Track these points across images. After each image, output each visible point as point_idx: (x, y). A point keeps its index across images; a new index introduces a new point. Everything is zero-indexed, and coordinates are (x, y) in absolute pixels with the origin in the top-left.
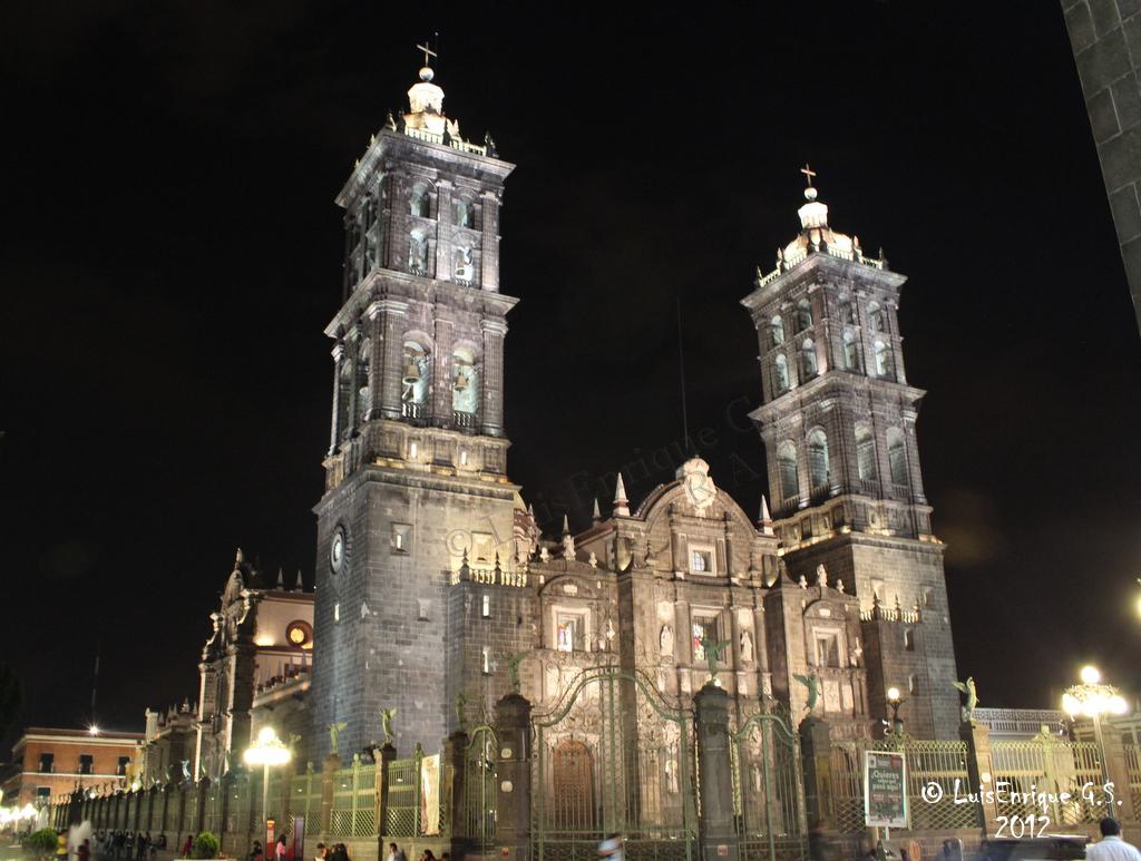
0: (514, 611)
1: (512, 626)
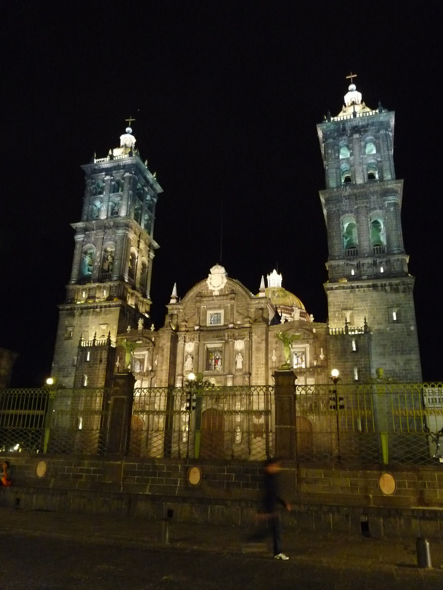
0: (99, 357)
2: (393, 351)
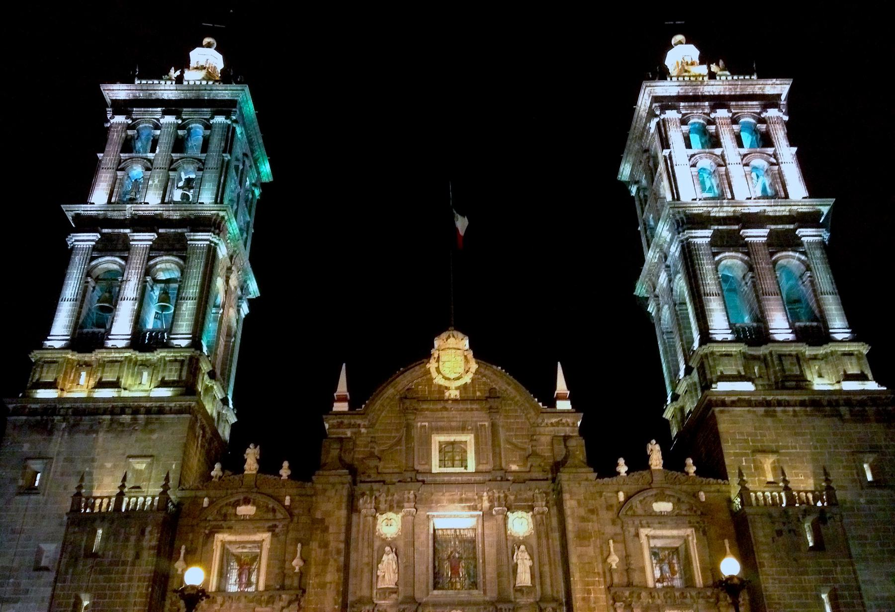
1: (124, 563)
2: (882, 552)
